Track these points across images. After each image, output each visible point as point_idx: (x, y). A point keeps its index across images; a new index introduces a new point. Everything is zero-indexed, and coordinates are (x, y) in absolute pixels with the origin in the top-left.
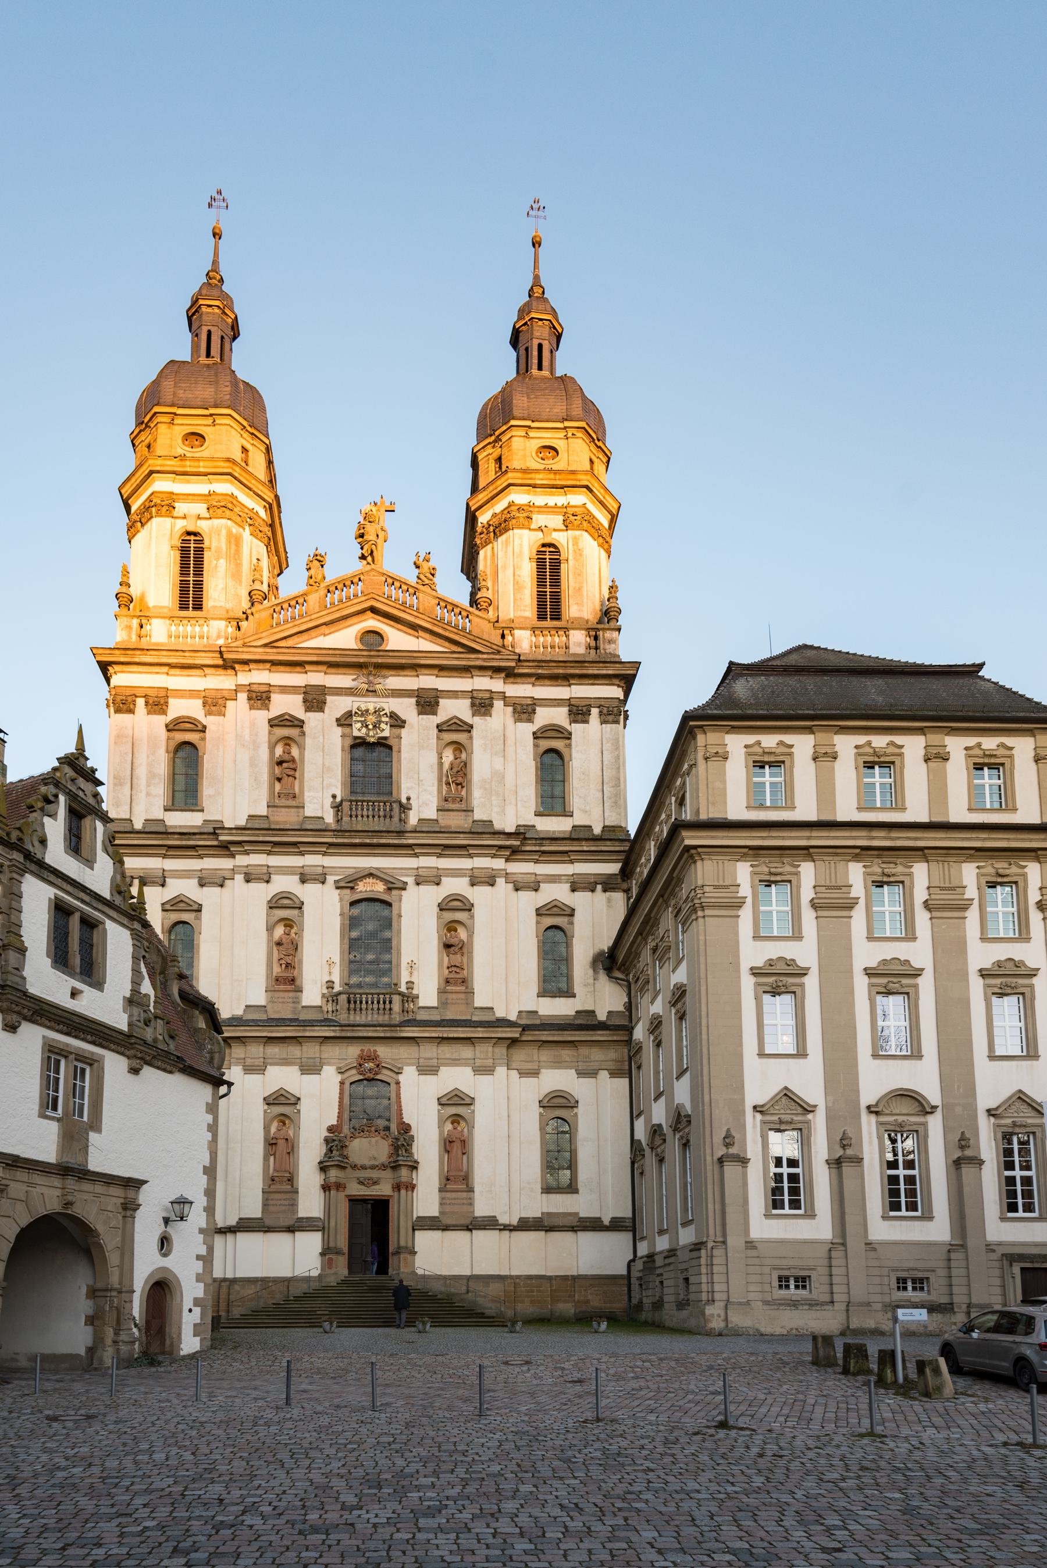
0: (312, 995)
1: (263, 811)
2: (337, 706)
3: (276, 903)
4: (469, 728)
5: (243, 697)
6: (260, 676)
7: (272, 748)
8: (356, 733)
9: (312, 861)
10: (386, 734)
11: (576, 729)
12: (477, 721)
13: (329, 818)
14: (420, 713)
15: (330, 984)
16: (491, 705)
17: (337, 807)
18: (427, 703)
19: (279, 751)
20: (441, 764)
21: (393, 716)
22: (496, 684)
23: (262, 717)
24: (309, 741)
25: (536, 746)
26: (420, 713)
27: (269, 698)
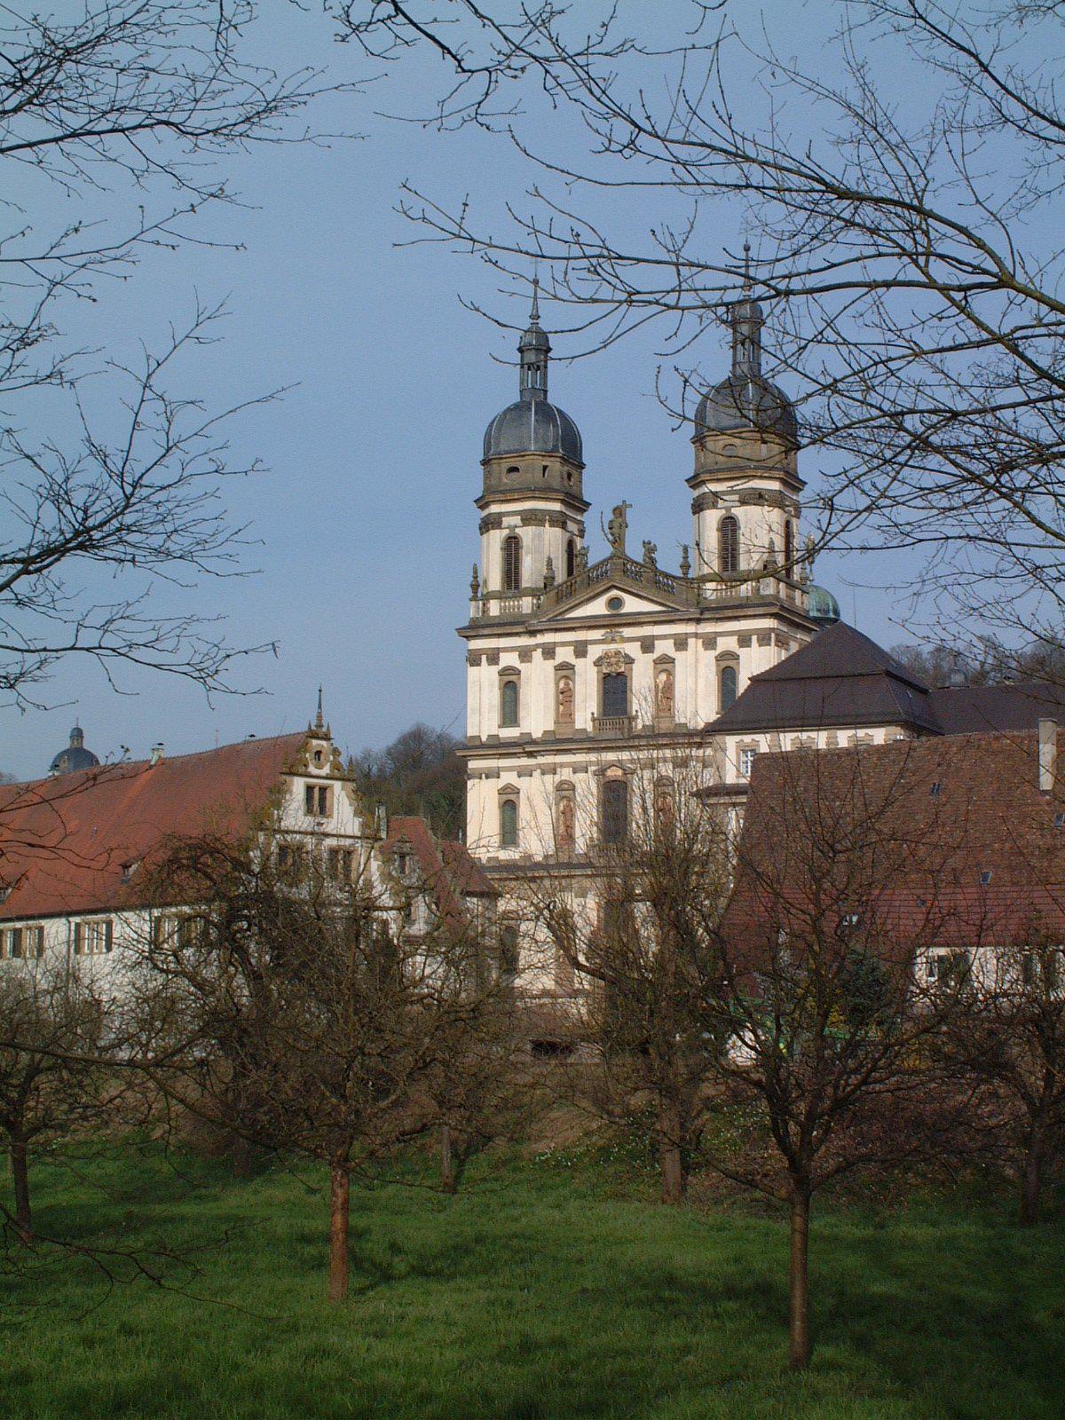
0: (581, 846)
1: (551, 727)
2: (595, 652)
3: (560, 787)
4: (672, 661)
5: (540, 650)
6: (549, 638)
7: (557, 684)
8: (605, 671)
9: (580, 758)
10: (622, 670)
11: (742, 652)
12: (678, 656)
13: (590, 728)
14: (643, 653)
15: (591, 839)
16: (687, 644)
17: (594, 720)
18: (647, 645)
19: (562, 685)
20: (657, 686)
21: (627, 656)
22: (690, 628)
23: (551, 664)
24: (577, 678)
25: (718, 666)
26: (643, 653)
27: (554, 652)
